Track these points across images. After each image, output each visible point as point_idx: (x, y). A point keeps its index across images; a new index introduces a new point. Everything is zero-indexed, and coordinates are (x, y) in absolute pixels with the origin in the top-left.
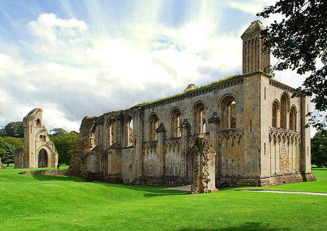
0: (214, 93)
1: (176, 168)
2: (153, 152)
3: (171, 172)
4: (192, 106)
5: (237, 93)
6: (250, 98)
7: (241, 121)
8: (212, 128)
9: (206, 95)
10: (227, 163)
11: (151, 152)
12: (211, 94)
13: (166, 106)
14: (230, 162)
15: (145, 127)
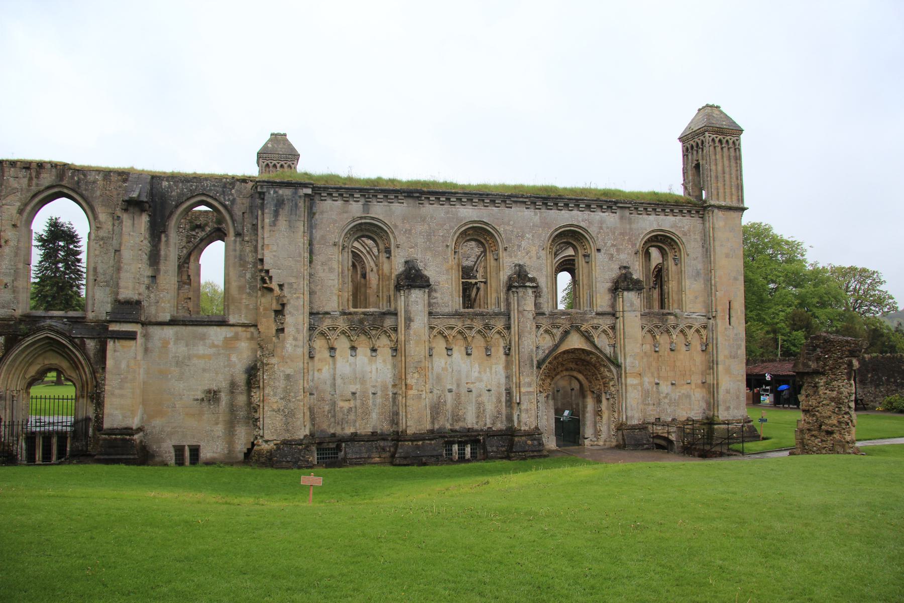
0: (622, 218)
1: (480, 405)
2: (363, 351)
3: (456, 418)
4: (546, 234)
5: (685, 234)
6: (727, 256)
7: (696, 298)
8: (632, 304)
9: (598, 215)
10: (658, 392)
11: (353, 348)
12: (610, 219)
13: (434, 211)
14: (665, 388)
15: (318, 259)
